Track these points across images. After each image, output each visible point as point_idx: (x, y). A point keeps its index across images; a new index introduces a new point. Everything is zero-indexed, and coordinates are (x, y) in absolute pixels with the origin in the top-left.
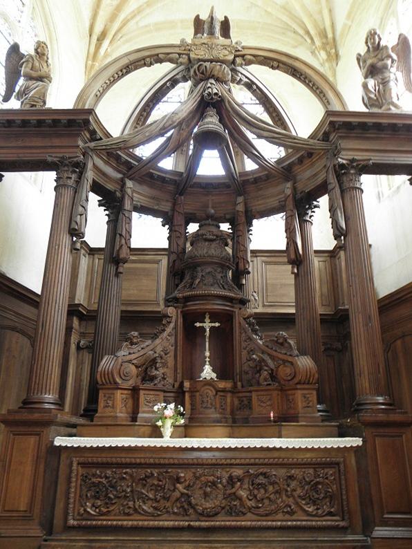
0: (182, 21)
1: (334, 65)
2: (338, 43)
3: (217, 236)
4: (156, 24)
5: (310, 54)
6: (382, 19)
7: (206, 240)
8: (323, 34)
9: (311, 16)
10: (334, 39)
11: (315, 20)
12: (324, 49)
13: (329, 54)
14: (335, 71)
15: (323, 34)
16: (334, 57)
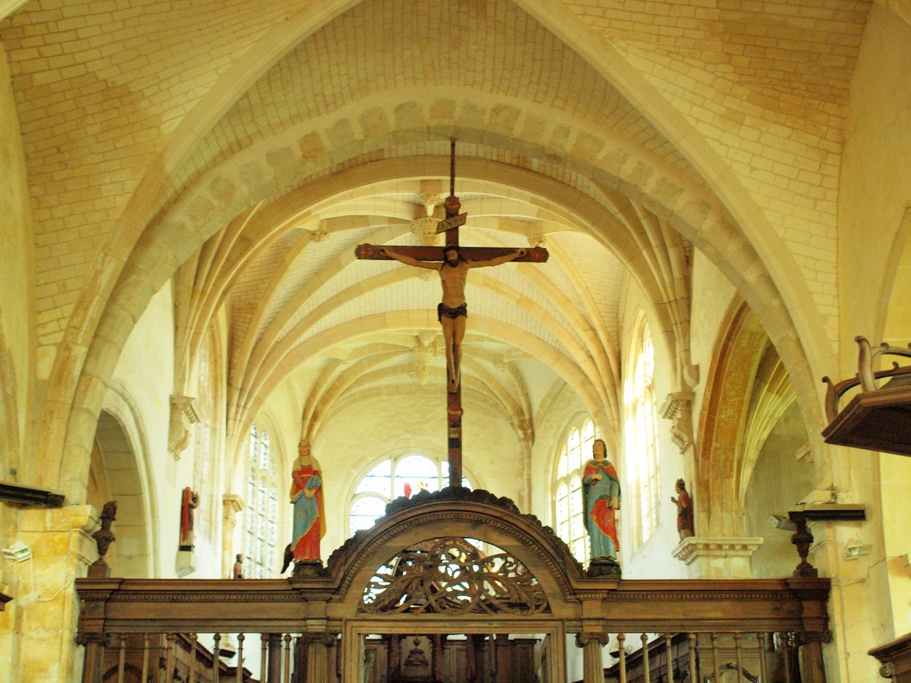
0: (387, 387)
1: (530, 443)
2: (535, 423)
3: (421, 662)
4: (362, 392)
5: (509, 426)
6: (559, 442)
7: (414, 665)
8: (520, 412)
9: (509, 396)
10: (531, 419)
11: (513, 400)
12: (522, 427)
13: (525, 434)
14: (530, 450)
15: (520, 412)
16: (530, 437)
